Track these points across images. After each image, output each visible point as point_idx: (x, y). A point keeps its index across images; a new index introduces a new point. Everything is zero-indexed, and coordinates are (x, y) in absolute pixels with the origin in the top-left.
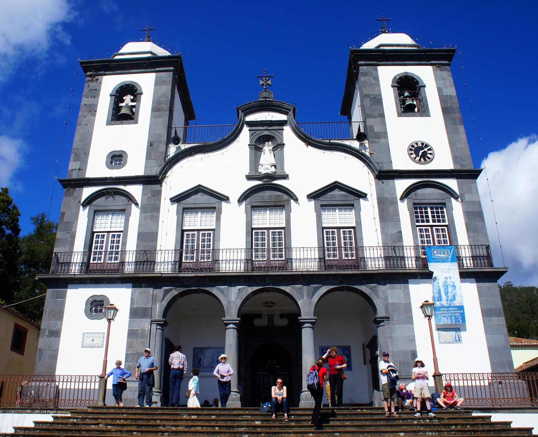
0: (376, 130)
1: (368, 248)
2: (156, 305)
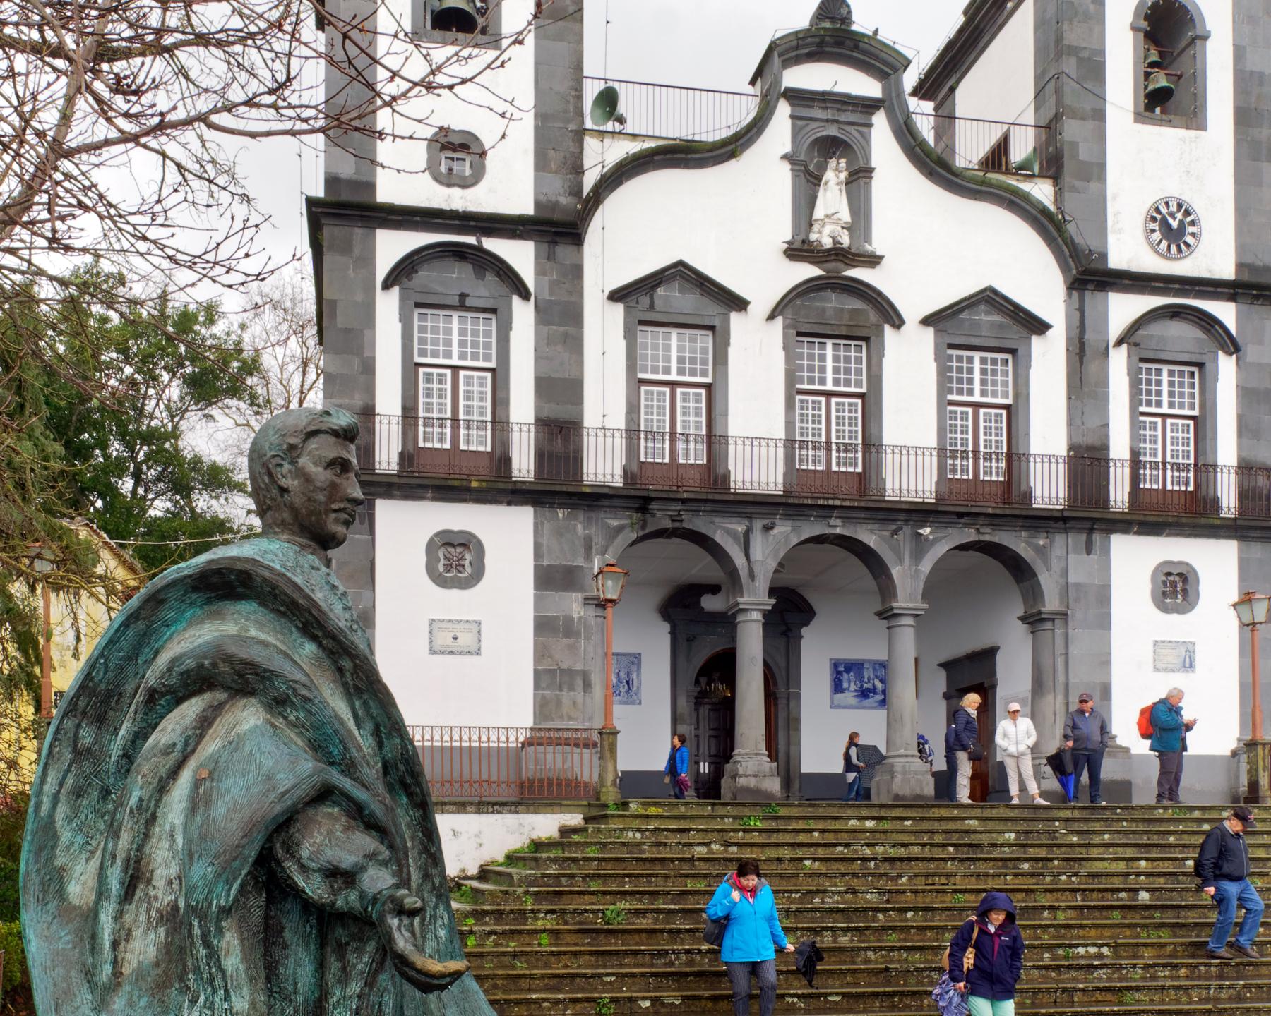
0: (1083, 155)
1: (1038, 460)
2: (592, 561)
